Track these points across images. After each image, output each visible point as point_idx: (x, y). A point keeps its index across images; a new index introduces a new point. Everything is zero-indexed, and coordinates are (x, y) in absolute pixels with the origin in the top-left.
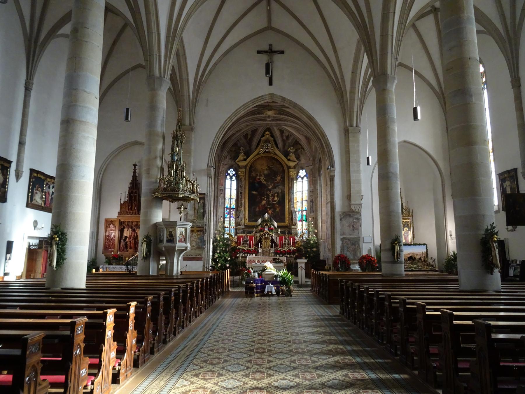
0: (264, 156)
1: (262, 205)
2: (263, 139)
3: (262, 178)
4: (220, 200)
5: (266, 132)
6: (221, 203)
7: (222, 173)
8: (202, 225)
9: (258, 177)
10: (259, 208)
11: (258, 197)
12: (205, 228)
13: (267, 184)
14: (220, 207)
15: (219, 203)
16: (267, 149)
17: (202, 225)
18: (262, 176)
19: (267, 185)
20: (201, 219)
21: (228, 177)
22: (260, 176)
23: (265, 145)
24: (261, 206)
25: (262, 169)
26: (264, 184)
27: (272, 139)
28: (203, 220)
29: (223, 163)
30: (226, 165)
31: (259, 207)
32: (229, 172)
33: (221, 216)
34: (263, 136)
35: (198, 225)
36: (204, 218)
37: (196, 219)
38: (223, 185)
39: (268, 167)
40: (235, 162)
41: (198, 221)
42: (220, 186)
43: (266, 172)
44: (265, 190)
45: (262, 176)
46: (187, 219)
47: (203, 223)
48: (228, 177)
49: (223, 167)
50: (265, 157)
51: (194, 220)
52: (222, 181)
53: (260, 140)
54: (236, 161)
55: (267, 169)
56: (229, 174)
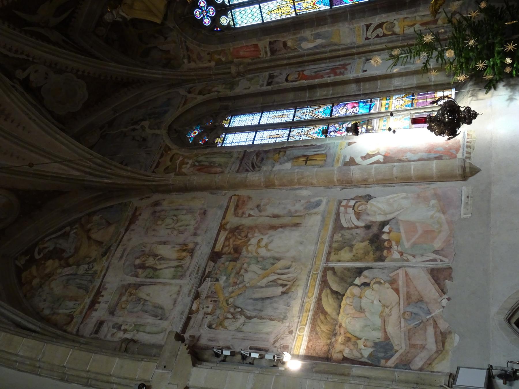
4: (307, 46)
6: (319, 41)
7: (216, 57)
14: (335, 40)
15: (322, 46)
21: (224, 21)
29: (186, 61)
30: (188, 49)
32: (207, 22)
33: (368, 26)
38: (256, 46)
40: (165, 17)
42: (263, 53)
48: (224, 21)
49: (200, 58)
52: (241, 53)
54: (158, 21)
56: (215, 20)
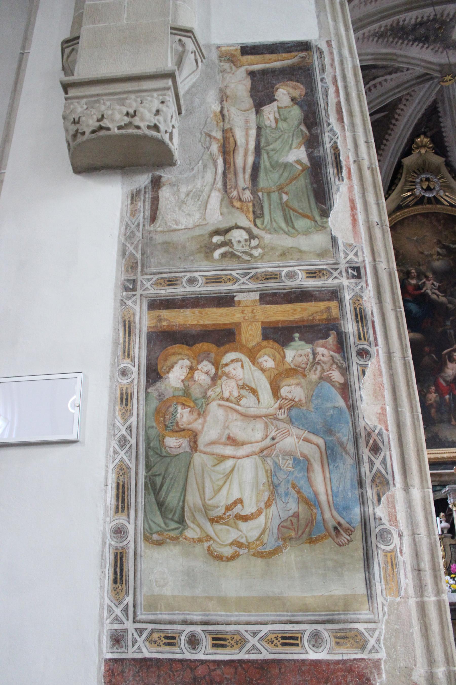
0: (423, 215)
1: (449, 379)
2: (407, 161)
3: (429, 284)
5: (418, 136)
8: (312, 274)
9: (414, 282)
10: (437, 391)
11: (427, 349)
12: (357, 299)
13: (450, 302)
16: (429, 189)
17: (312, 274)
18: (427, 277)
19: (450, 306)
20: (301, 224)
22: (419, 278)
23: (418, 180)
24: (444, 383)
25: (422, 253)
26: (441, 304)
27: (438, 160)
28: (323, 227)
31: (437, 385)
34: (407, 152)
35: (268, 277)
36: (325, 214)
37: (244, 221)
39: (444, 247)
41: (268, 238)
43: (438, 264)
44: (448, 323)
45: (427, 277)
46: (159, 225)
47: (322, 255)
50: (425, 215)
51: (217, 232)
53: (399, 166)
55: (439, 254)
